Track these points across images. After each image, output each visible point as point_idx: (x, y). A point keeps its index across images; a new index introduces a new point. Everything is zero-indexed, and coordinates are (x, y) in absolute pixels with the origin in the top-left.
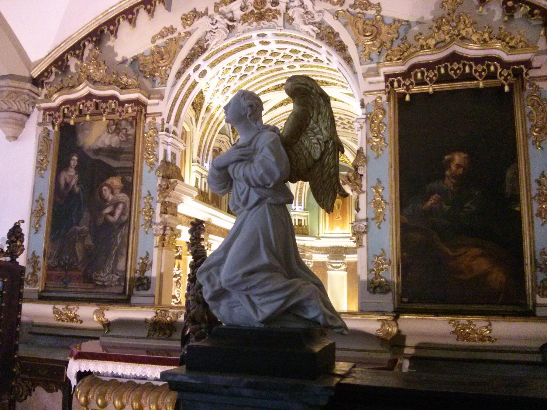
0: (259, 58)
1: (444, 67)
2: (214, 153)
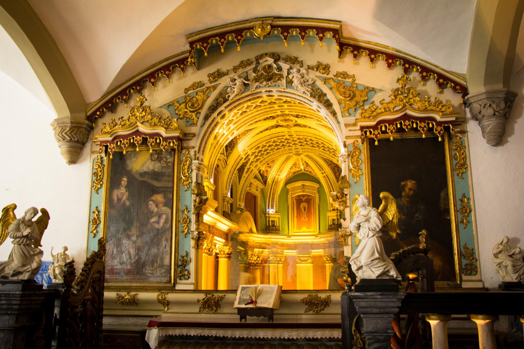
1: (399, 123)
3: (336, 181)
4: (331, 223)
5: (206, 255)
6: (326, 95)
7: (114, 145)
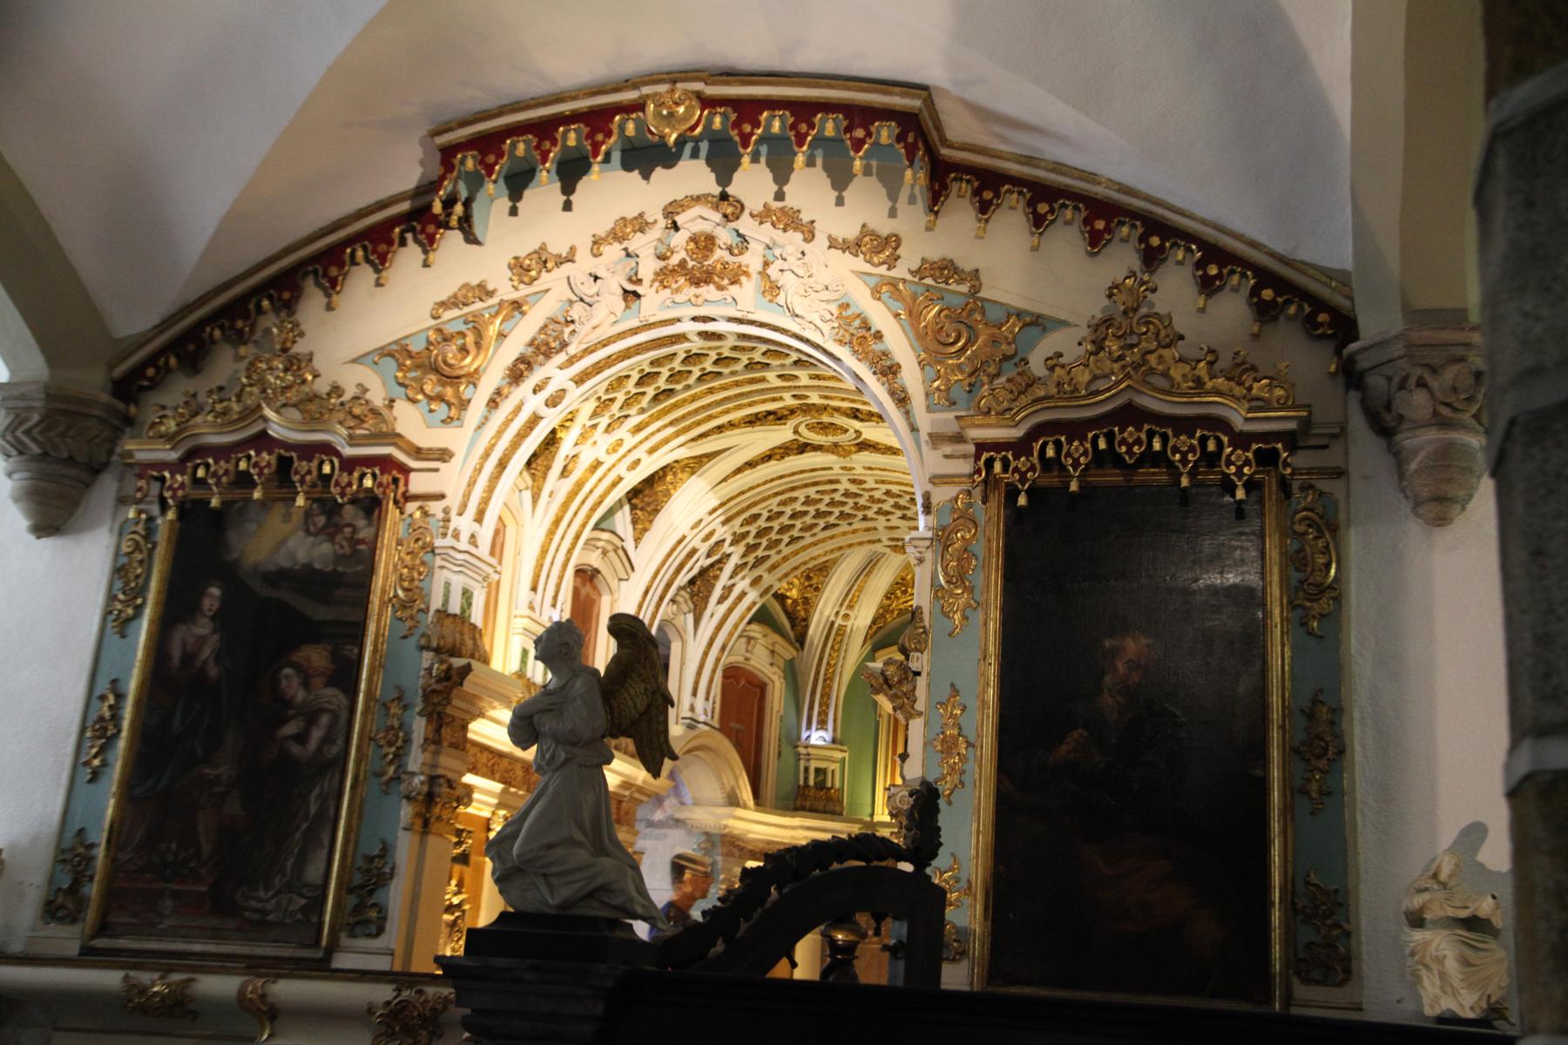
0: (703, 355)
1: (1106, 435)
2: (579, 580)
6: (878, 336)
7: (185, 477)
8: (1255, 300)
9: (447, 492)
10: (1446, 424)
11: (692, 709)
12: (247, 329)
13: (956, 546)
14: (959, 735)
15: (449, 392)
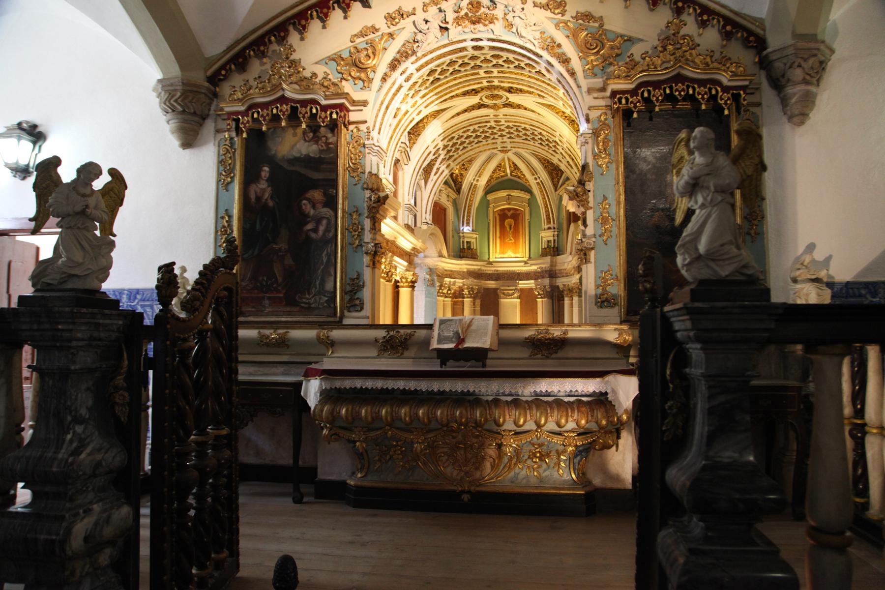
1: (669, 87)
3: (553, 191)
4: (545, 245)
5: (384, 281)
6: (559, 46)
8: (724, 30)
9: (368, 121)
10: (806, 82)
11: (426, 219)
12: (266, 50)
13: (602, 137)
14: (609, 216)
15: (363, 75)
